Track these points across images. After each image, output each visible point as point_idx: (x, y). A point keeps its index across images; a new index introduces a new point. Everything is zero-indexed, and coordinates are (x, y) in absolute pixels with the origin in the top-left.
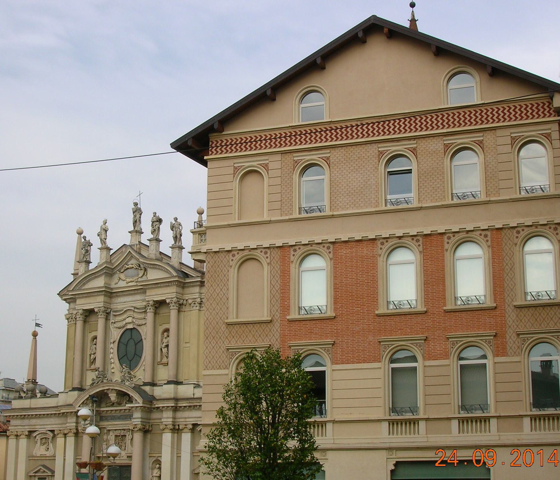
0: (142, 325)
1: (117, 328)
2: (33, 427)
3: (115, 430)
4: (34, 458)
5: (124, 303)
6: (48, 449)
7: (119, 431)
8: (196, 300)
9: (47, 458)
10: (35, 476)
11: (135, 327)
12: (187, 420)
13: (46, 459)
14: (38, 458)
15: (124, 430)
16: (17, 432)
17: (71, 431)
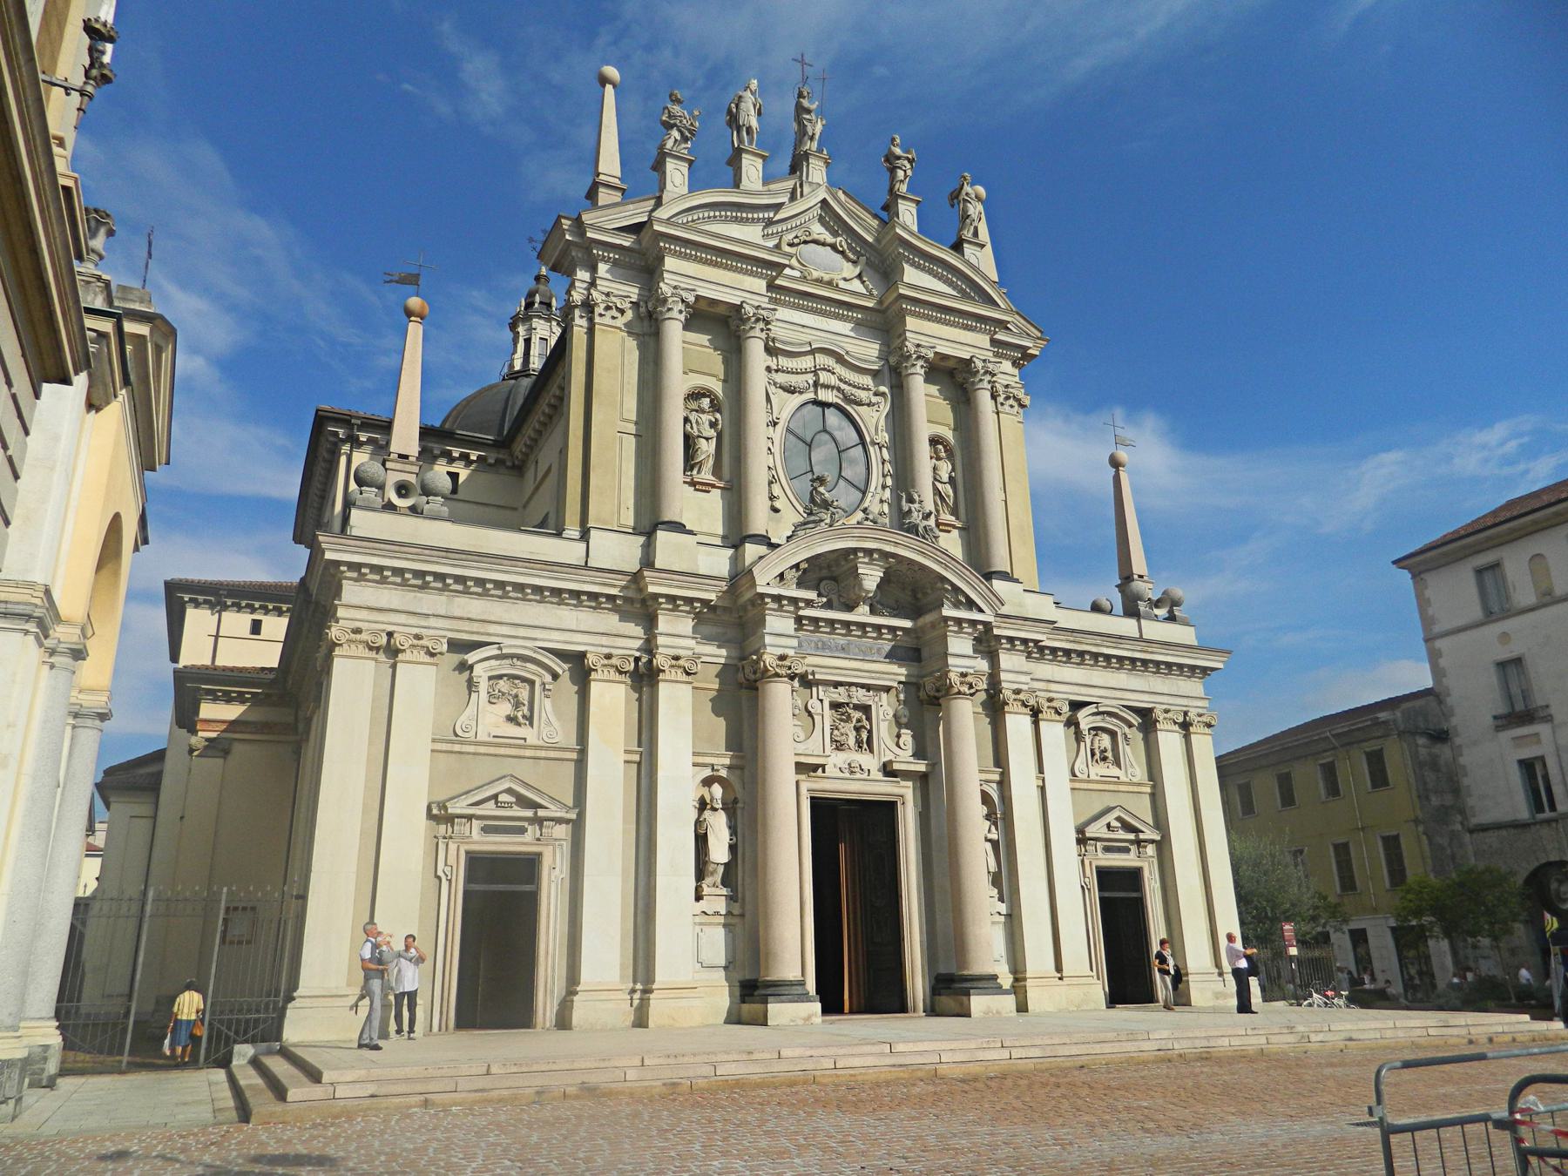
0: (863, 405)
1: (781, 387)
2: (475, 627)
3: (837, 685)
4: (457, 748)
5: (802, 330)
6: (530, 719)
7: (853, 689)
8: (1011, 390)
9: (528, 753)
10: (470, 818)
11: (840, 402)
12: (1053, 687)
13: (524, 757)
14: (482, 749)
15: (868, 687)
16: (390, 635)
17: (681, 662)
